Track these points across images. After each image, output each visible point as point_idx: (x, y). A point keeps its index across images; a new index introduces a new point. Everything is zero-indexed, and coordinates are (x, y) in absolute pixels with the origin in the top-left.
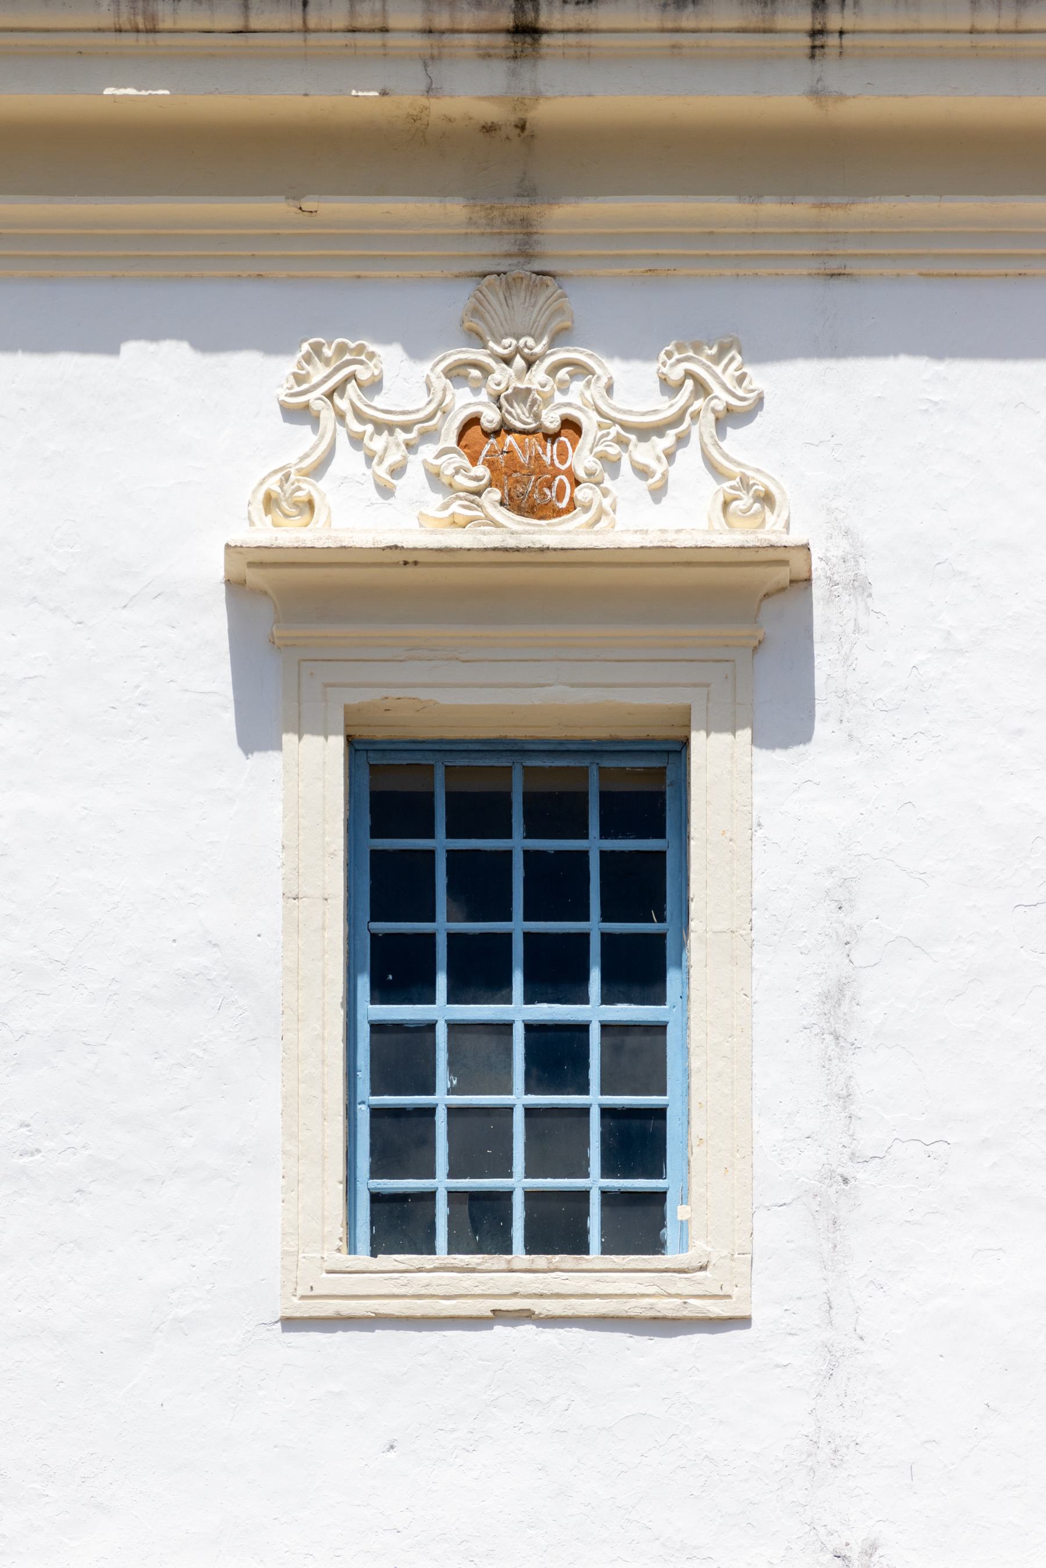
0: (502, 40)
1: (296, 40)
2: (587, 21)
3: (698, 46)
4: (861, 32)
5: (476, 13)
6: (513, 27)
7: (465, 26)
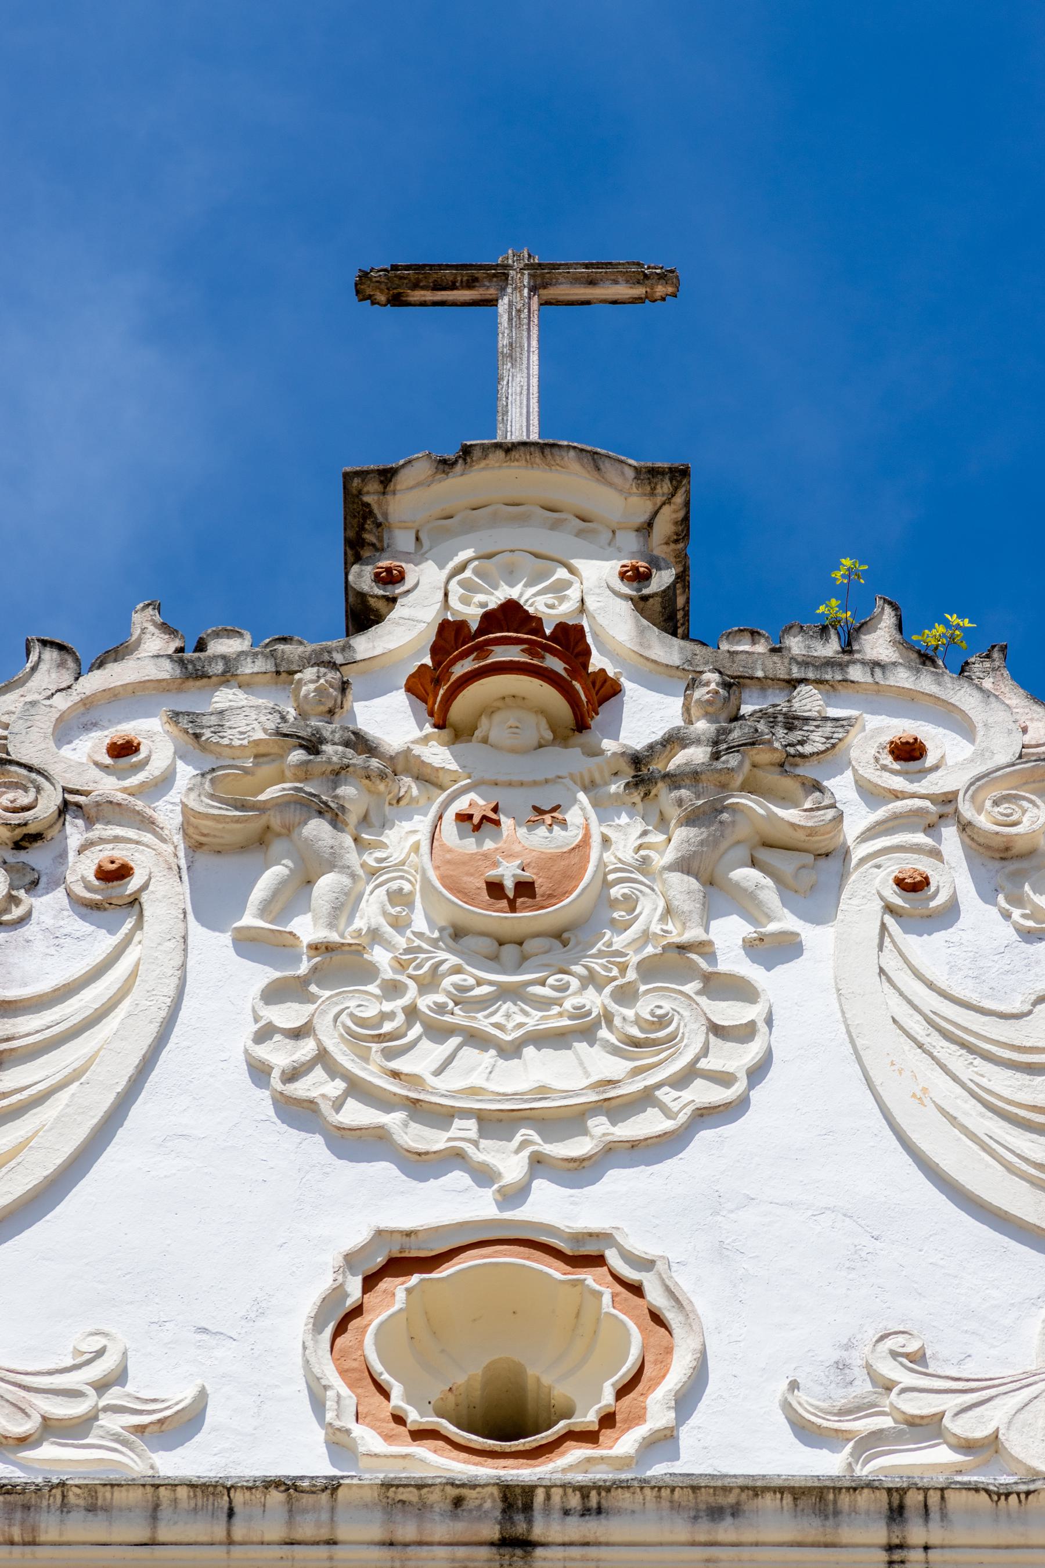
0: (484, 1552)
1: (219, 1552)
2: (595, 1533)
3: (740, 1560)
4: (951, 1547)
5: (451, 1524)
6: (499, 1540)
7: (437, 1538)
